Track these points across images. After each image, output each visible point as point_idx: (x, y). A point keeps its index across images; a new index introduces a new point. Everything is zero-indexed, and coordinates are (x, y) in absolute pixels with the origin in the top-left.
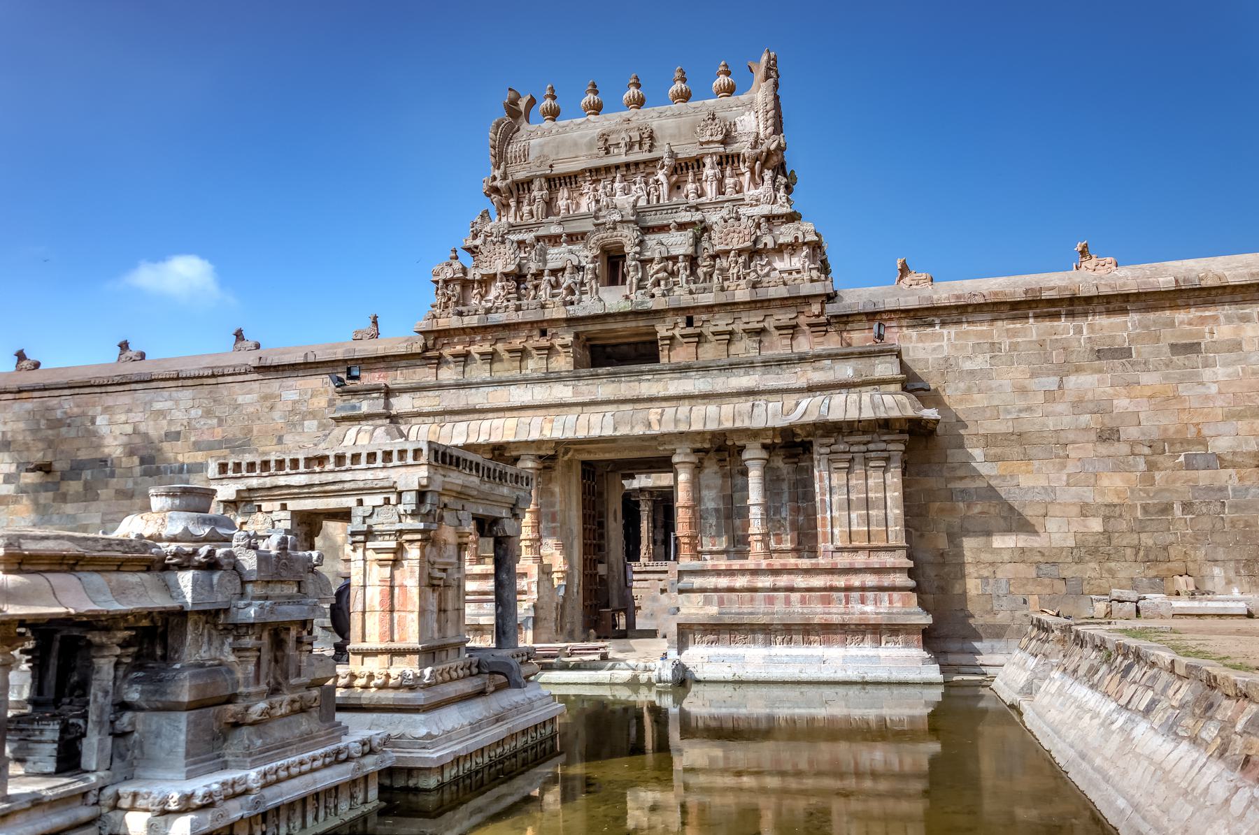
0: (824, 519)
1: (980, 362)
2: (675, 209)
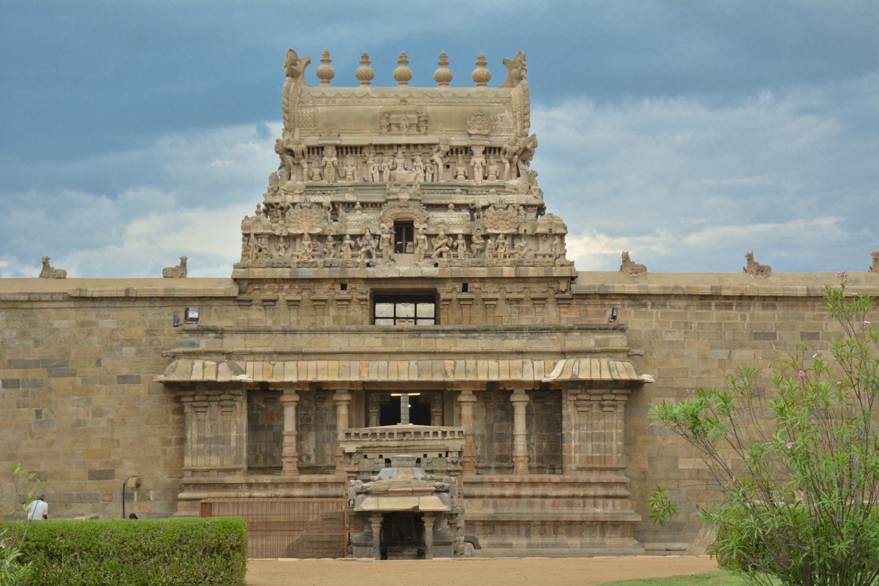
0: (570, 447)
1: (676, 336)
2: (450, 188)
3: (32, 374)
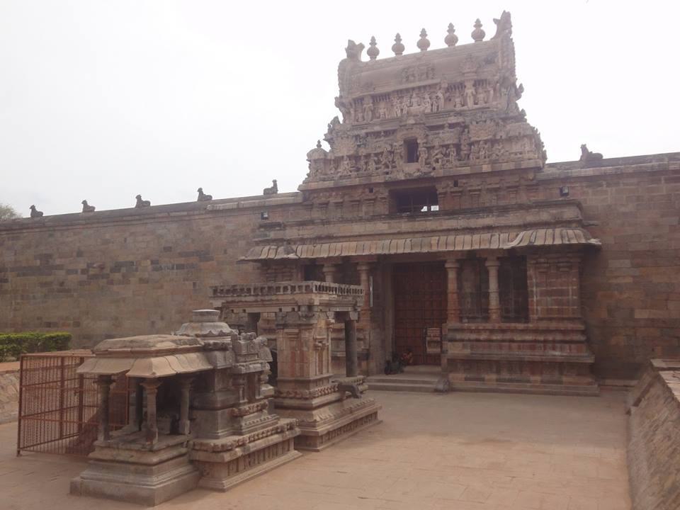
2: (448, 113)
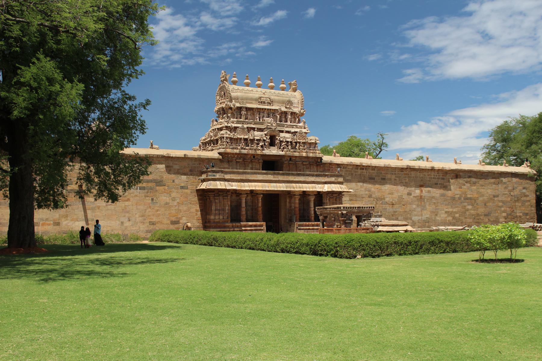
3: (150, 185)
